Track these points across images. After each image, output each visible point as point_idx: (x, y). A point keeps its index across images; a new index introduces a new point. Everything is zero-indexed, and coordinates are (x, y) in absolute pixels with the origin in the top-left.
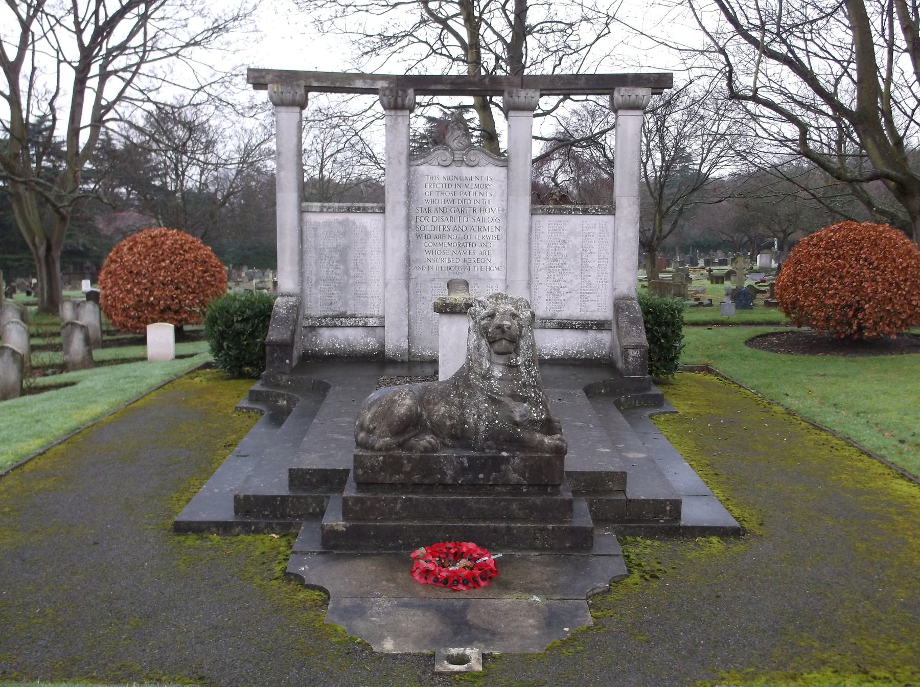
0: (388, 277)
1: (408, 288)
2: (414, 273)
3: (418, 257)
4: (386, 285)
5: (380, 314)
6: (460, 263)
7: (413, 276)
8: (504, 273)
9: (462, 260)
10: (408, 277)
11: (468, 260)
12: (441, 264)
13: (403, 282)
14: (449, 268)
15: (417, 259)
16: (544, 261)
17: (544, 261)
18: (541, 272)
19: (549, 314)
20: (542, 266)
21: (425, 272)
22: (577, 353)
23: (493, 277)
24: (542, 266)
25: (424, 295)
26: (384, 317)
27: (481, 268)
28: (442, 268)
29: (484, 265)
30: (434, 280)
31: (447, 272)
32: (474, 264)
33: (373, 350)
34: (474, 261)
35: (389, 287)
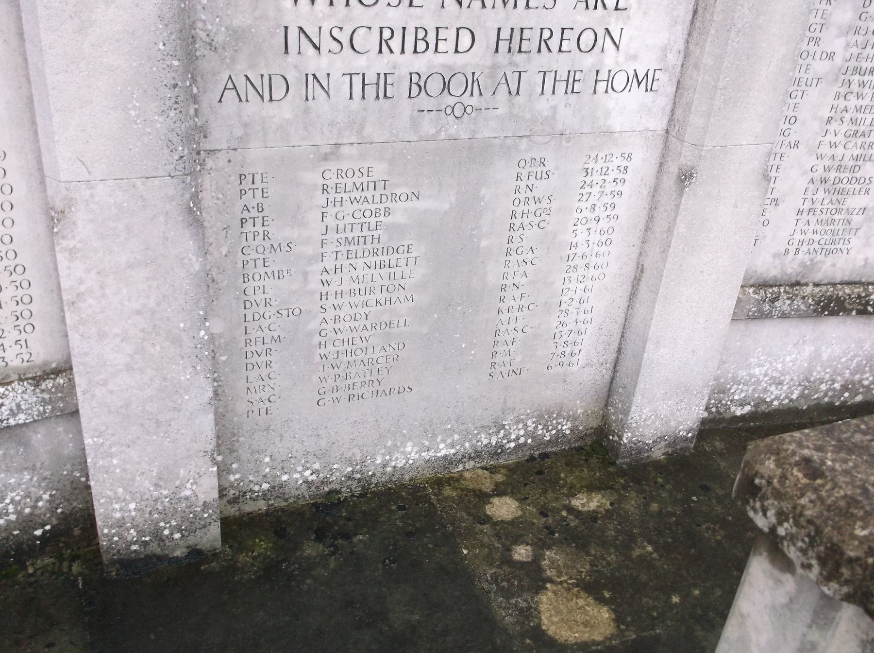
0: (64, 165)
1: (193, 215)
2: (226, 118)
3: (241, 20)
4: (54, 219)
5: (41, 351)
6: (477, 59)
7: (219, 138)
8: (662, 101)
9: (485, 40)
10: (194, 150)
11: (512, 41)
12: (372, 64)
13: (165, 192)
14: (418, 85)
15: (238, 35)
16: (837, 45)
17: (837, 45)
18: (813, 93)
19: (791, 267)
20: (820, 67)
21: (284, 111)
22: (845, 388)
23: (616, 123)
24: (820, 67)
25: (279, 233)
26: (64, 369)
27: (572, 81)
28: (382, 86)
29: (587, 62)
30: (334, 151)
31: (406, 107)
32: (545, 60)
33: (28, 523)
34: (544, 44)
35: (82, 227)
